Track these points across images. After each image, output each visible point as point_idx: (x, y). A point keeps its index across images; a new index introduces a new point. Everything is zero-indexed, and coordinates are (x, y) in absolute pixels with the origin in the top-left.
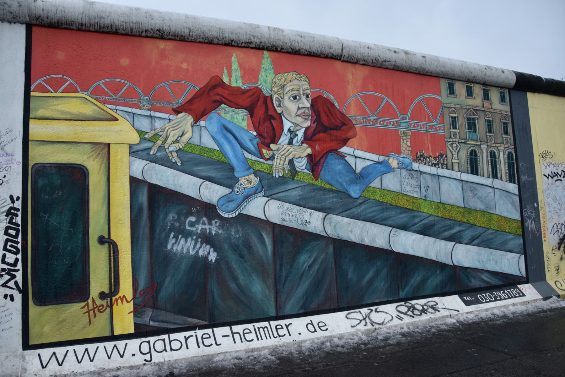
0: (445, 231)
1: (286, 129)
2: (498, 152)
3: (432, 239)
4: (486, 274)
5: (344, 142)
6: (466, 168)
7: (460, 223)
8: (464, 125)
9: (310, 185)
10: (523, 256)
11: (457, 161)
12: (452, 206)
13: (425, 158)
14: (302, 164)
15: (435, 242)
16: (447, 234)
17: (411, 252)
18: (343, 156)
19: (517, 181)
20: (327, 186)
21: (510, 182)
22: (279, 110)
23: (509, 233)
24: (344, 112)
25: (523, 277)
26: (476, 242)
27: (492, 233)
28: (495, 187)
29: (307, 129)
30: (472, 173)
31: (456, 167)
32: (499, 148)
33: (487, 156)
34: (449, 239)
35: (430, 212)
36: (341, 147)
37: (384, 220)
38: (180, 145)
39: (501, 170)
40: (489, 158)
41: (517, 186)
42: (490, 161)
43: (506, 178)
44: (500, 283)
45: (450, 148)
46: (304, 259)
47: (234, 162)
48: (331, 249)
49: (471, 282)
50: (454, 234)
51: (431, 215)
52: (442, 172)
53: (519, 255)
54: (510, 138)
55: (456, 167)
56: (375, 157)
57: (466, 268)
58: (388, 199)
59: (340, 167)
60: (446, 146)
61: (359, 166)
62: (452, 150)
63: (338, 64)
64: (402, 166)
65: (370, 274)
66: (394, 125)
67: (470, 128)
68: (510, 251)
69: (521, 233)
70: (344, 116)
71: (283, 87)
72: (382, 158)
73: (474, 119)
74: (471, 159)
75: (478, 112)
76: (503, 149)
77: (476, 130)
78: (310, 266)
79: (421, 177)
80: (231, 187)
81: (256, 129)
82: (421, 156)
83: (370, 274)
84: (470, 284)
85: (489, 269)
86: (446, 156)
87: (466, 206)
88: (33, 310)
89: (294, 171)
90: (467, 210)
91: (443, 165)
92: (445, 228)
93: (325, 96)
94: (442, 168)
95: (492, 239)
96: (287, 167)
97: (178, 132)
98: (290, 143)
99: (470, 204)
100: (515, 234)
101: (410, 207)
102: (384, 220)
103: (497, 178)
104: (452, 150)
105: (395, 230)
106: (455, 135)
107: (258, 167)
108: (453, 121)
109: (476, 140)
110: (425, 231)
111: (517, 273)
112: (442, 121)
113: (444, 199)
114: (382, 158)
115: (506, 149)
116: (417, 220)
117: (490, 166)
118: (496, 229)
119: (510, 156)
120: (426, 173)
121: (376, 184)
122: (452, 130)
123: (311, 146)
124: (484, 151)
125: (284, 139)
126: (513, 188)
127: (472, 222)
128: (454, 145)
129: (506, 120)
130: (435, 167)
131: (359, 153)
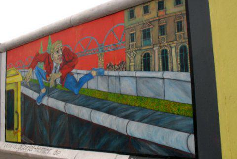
0: (124, 112)
1: (54, 66)
2: (170, 49)
3: (114, 117)
4: (153, 146)
5: (73, 67)
6: (140, 67)
7: (134, 107)
8: (140, 38)
9: (61, 90)
10: (192, 137)
11: (134, 64)
12: (128, 95)
13: (112, 67)
14: (58, 81)
15: (115, 119)
16: (124, 114)
17: (102, 124)
18: (72, 75)
19: (189, 69)
20: (66, 90)
21: (182, 71)
22: (52, 59)
23: (178, 115)
24: (74, 52)
25: (191, 154)
26: (146, 120)
27: (161, 115)
28: (165, 77)
29: (61, 64)
30: (145, 70)
31: (132, 68)
32: (171, 45)
33: (159, 55)
34: (125, 117)
35: (113, 100)
36: (72, 70)
37: (89, 105)
38: (29, 80)
39: (172, 63)
40: (160, 56)
41: (188, 74)
42: (161, 58)
43: (178, 69)
44: (167, 154)
45: (129, 55)
46: (59, 123)
47: (41, 84)
48: (67, 119)
49: (140, 149)
50: (129, 114)
51: (114, 102)
52: (122, 73)
53: (187, 134)
54: (184, 34)
55: (132, 68)
56: (85, 72)
57: (135, 139)
58: (90, 94)
59: (71, 80)
60: (125, 55)
61: (78, 78)
62: (129, 57)
63: (73, 29)
64: (100, 74)
65: (82, 133)
66: (95, 51)
67: (145, 37)
68: (178, 130)
69: (192, 115)
70: (74, 54)
71: (54, 49)
72: (88, 72)
73: (148, 30)
74: (144, 60)
75: (152, 23)
76: (175, 44)
77: (150, 36)
78: (60, 126)
79: (109, 80)
80: (39, 93)
81: (46, 69)
82: (109, 66)
83: (82, 133)
84: (139, 150)
85: (156, 142)
86: (126, 62)
87: (139, 94)
88: (7, 131)
89: (56, 85)
90: (140, 98)
91: (123, 69)
92: (122, 110)
93: (67, 47)
94: (123, 71)
95: (159, 119)
96: (54, 83)
97: (28, 76)
98: (55, 72)
99: (142, 93)
100: (184, 116)
101: (102, 98)
102: (89, 105)
103: (168, 70)
104: (129, 57)
105: (93, 111)
106: (133, 46)
107: (46, 85)
108: (132, 37)
109: (150, 45)
110: (109, 112)
111: (186, 150)
112: (124, 40)
113: (123, 91)
114: (88, 72)
115: (178, 44)
116: (105, 106)
117: (161, 62)
118: (164, 111)
119: (183, 49)
120: (111, 76)
121: (85, 86)
122: (131, 43)
123: (61, 72)
124: (156, 51)
125: (54, 71)
126: (186, 76)
127: (143, 106)
128: (132, 53)
129: (181, 19)
130: (118, 70)
131: (79, 71)
